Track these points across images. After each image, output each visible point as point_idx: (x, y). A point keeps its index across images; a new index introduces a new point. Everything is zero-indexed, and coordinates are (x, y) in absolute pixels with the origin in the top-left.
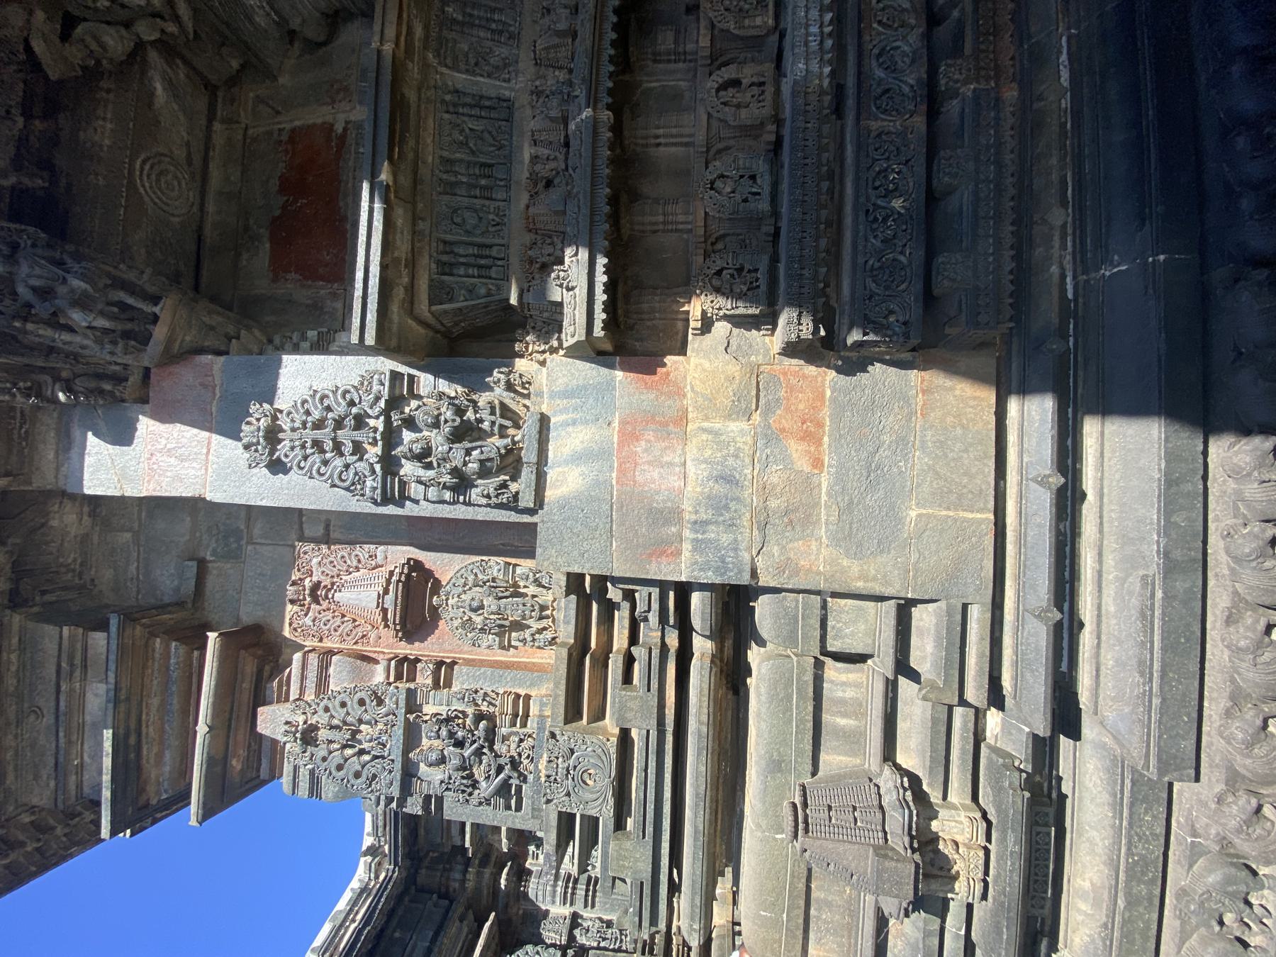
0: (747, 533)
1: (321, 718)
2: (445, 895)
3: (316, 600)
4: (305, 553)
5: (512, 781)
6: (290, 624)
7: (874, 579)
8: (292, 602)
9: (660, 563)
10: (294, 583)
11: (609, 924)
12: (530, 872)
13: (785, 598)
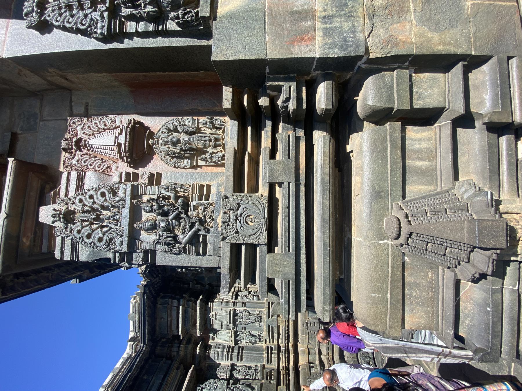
0: (362, 23)
1: (78, 207)
2: (170, 358)
3: (79, 148)
4: (74, 123)
5: (200, 233)
6: (64, 164)
7: (450, 44)
8: (65, 150)
9: (300, 46)
10: (66, 139)
11: (250, 368)
12: (211, 346)
13: (383, 75)
